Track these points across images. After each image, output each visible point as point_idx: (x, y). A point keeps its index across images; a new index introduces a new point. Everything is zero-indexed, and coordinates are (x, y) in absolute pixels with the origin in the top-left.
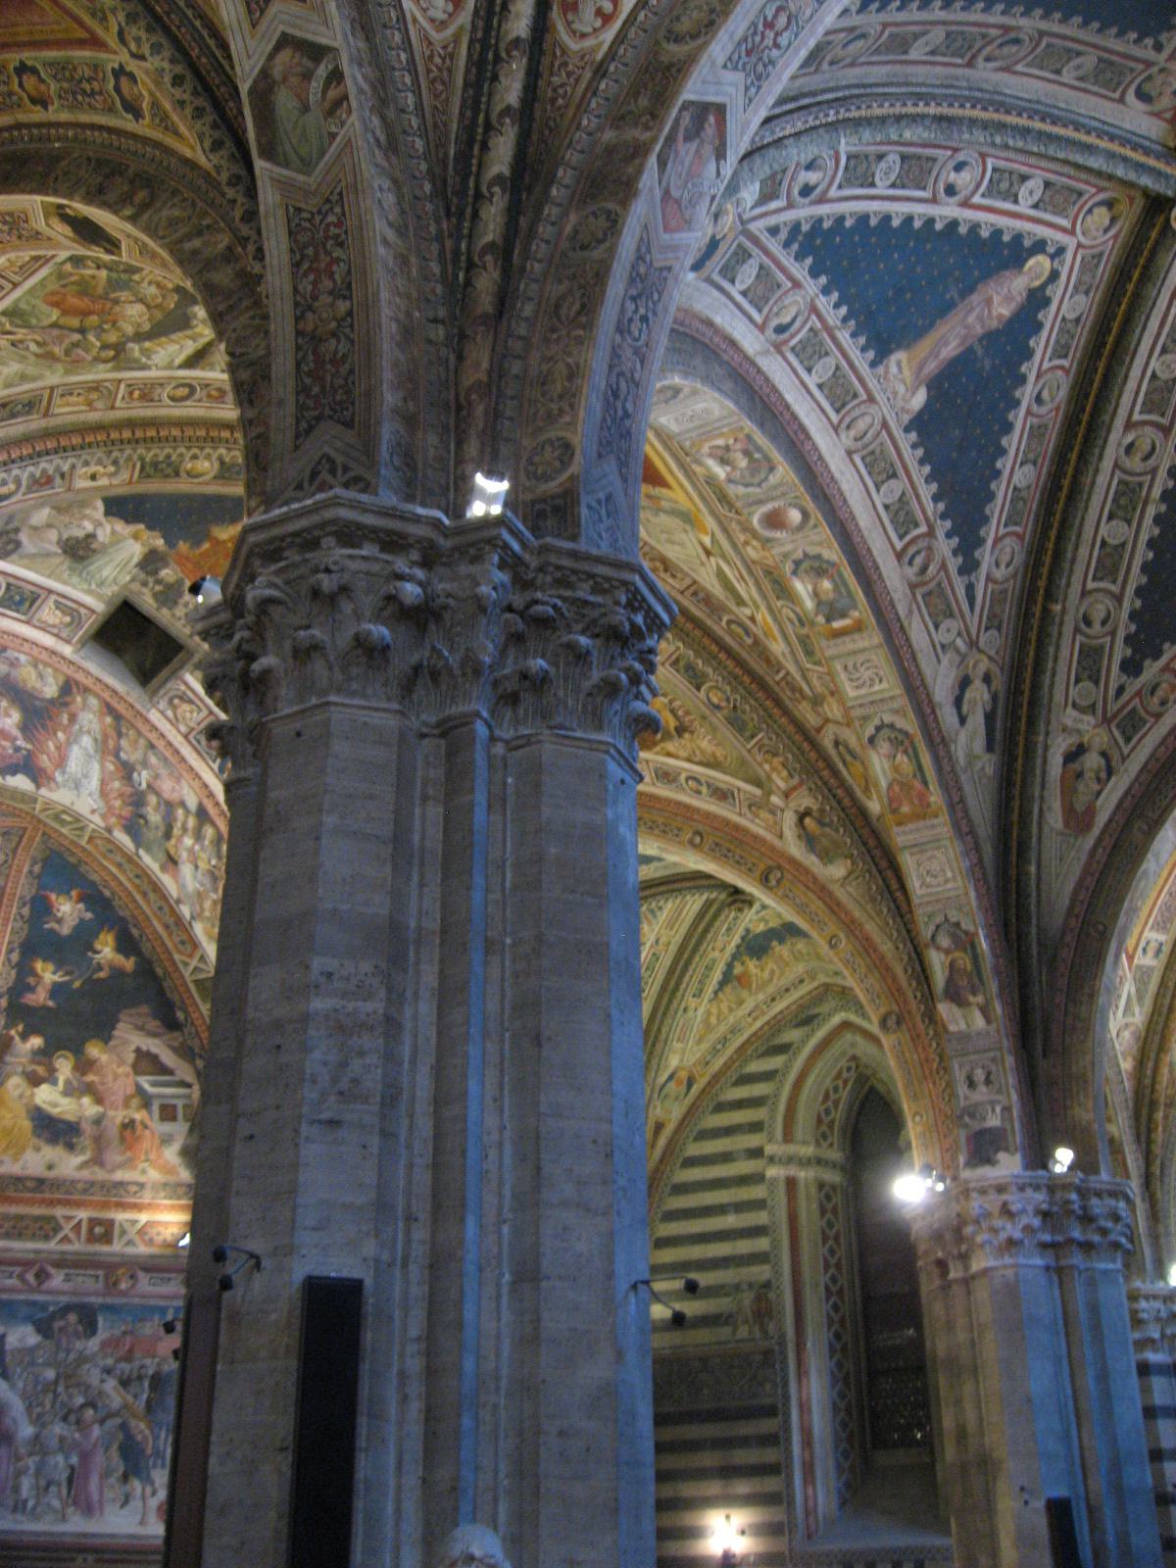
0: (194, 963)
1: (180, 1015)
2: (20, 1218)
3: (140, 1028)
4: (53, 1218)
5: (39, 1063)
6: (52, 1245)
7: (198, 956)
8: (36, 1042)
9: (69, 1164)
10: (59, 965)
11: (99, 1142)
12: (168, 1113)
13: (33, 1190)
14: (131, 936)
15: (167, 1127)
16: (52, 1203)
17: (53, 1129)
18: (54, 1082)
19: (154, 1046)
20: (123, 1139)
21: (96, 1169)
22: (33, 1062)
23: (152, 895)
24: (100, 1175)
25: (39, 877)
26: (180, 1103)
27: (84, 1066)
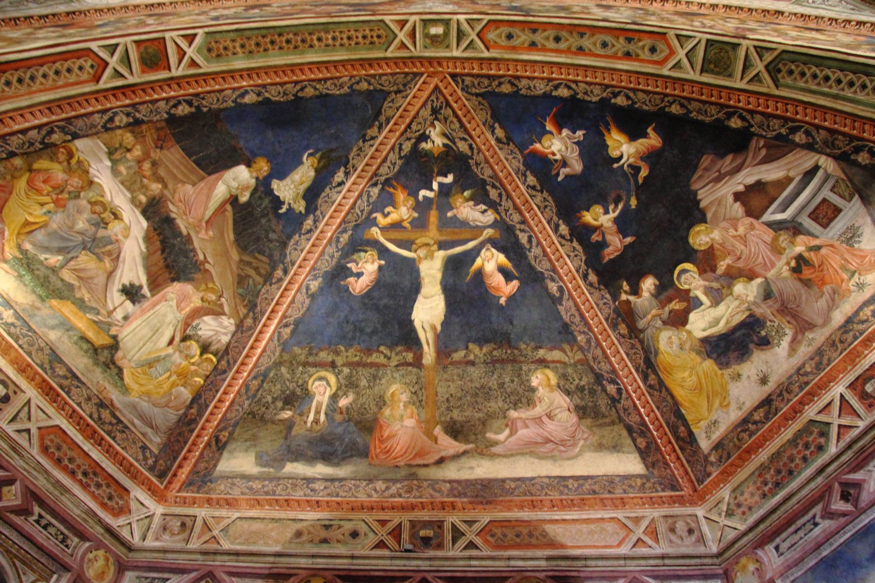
0: (681, 54)
1: (735, 123)
2: (776, 456)
3: (718, 180)
4: (812, 422)
5: (670, 300)
6: (833, 449)
7: (675, 43)
8: (648, 284)
9: (778, 360)
10: (603, 200)
11: (788, 310)
12: (825, 214)
13: (767, 418)
14: (620, 108)
15: (839, 225)
16: (796, 411)
17: (734, 345)
18: (698, 303)
19: (748, 177)
20: (807, 283)
21: (810, 335)
22: (663, 305)
23: (586, 43)
24: (818, 337)
25: (509, 139)
26: (826, 193)
27: (706, 262)
